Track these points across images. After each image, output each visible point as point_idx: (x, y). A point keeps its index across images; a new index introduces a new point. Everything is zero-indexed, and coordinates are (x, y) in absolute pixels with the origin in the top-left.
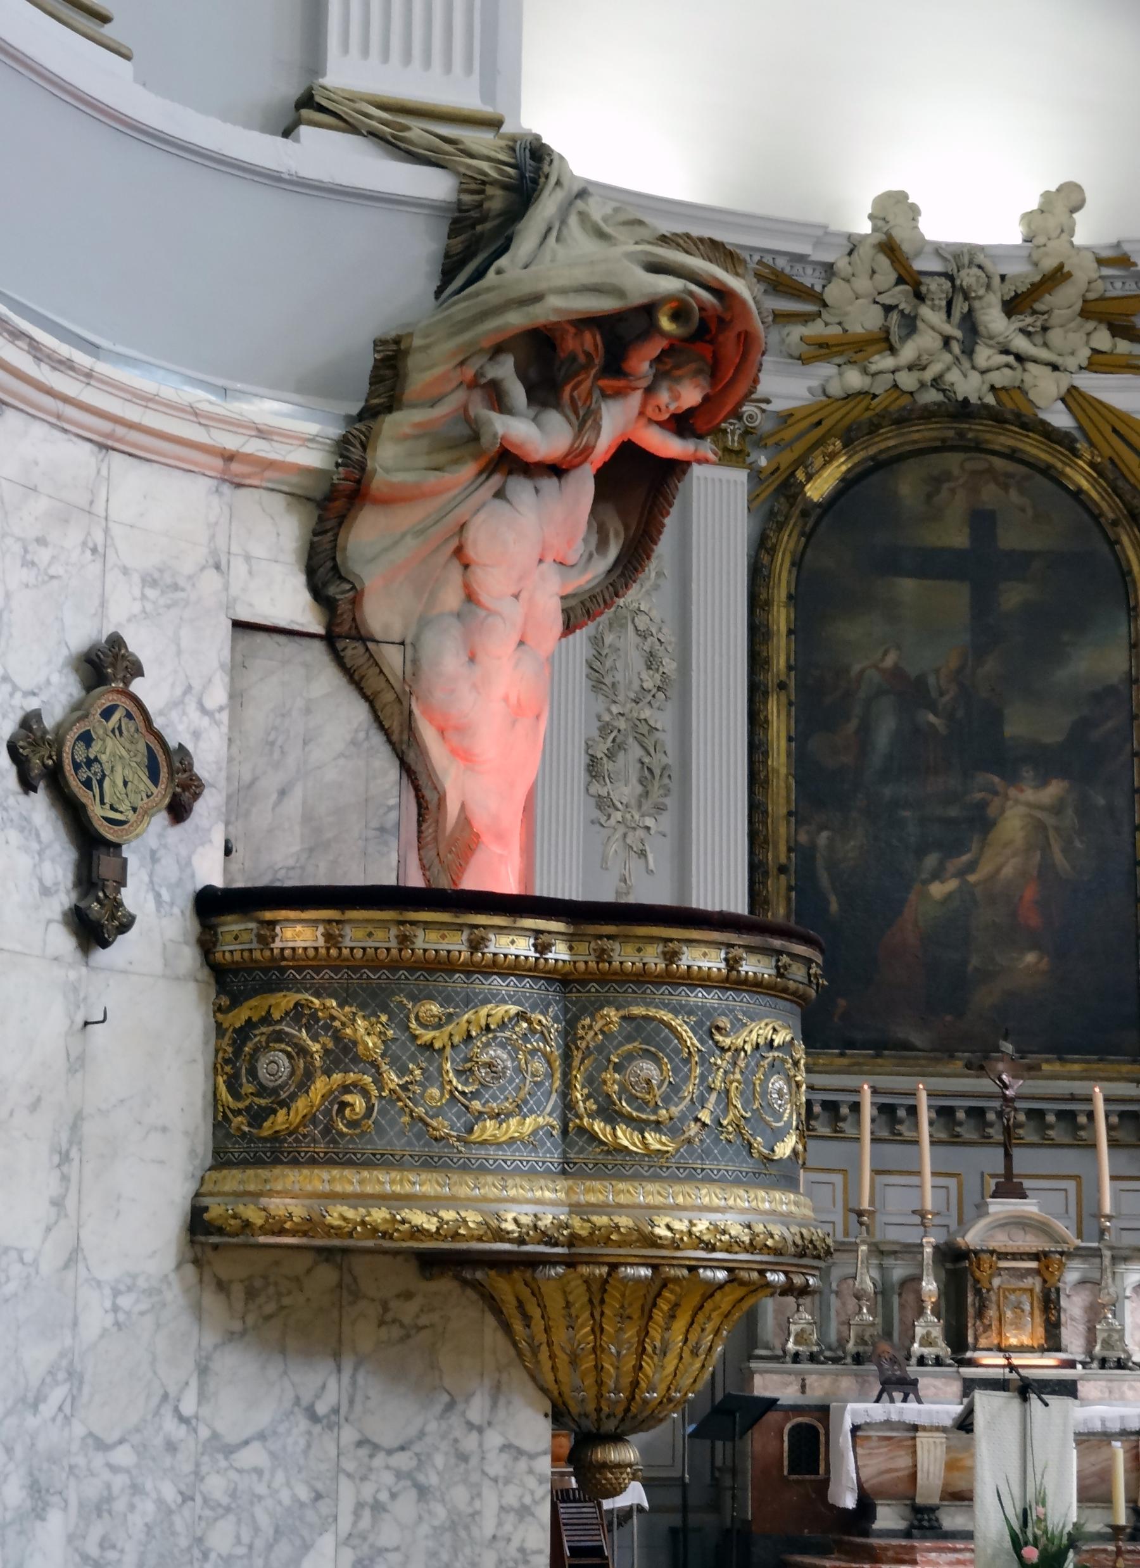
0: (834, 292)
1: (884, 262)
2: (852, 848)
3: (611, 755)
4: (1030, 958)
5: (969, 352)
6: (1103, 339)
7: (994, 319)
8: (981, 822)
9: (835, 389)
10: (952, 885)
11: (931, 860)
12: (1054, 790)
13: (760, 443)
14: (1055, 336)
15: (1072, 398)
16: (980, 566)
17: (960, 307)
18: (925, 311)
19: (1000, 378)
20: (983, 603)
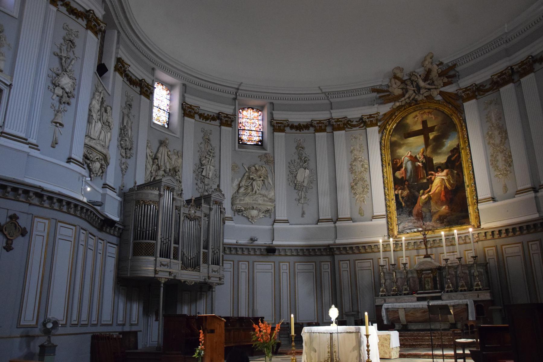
0: (390, 89)
1: (397, 81)
2: (406, 193)
3: (356, 184)
4: (444, 207)
5: (419, 92)
6: (446, 80)
7: (422, 84)
8: (431, 182)
9: (395, 107)
10: (426, 196)
11: (421, 191)
12: (445, 171)
13: (380, 121)
14: (436, 83)
15: (441, 93)
16: (425, 131)
17: (415, 84)
18: (408, 87)
19: (426, 95)
20: (427, 139)
